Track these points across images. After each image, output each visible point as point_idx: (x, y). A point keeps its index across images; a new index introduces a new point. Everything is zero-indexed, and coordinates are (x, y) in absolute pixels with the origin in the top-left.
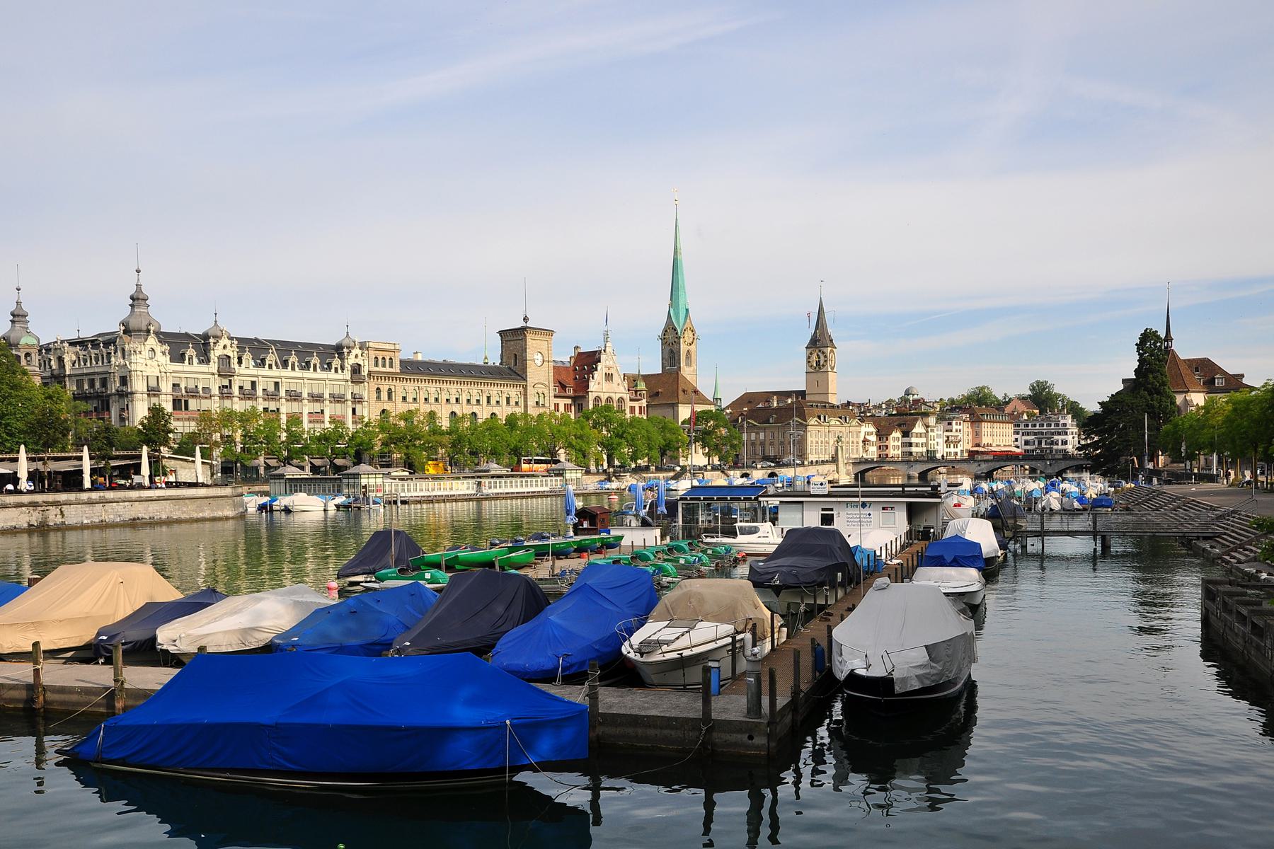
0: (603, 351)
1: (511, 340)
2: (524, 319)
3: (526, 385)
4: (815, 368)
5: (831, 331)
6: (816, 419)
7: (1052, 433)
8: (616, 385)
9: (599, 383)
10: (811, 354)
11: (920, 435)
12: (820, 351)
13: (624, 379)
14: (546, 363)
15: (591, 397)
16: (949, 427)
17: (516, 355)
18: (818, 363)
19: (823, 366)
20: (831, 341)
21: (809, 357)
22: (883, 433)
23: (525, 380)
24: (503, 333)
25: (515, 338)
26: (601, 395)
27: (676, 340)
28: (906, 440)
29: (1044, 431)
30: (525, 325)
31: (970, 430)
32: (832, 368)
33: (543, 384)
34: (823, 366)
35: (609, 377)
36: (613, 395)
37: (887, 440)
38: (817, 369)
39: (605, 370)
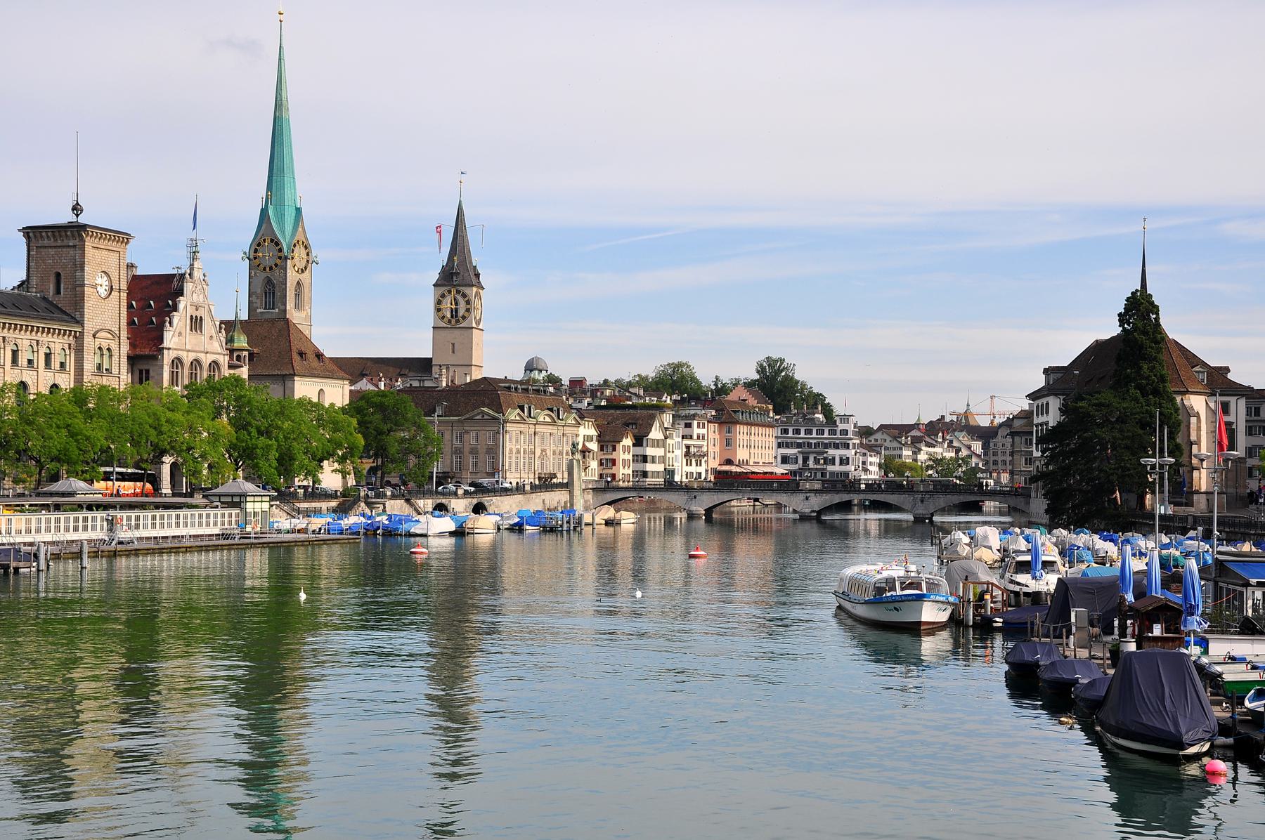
0: (187, 276)
1: (51, 247)
2: (74, 208)
3: (82, 333)
4: (450, 321)
5: (477, 258)
6: (518, 410)
7: (826, 446)
8: (207, 339)
9: (180, 334)
10: (443, 296)
11: (657, 444)
12: (458, 292)
13: (220, 328)
14: (115, 294)
15: (168, 357)
16: (687, 431)
17: (58, 275)
18: (455, 313)
19: (464, 317)
20: (477, 275)
21: (439, 302)
22: (607, 438)
23: (80, 323)
24: (32, 233)
25: (59, 243)
26: (183, 355)
27: (278, 262)
28: (639, 450)
29: (813, 441)
31: (717, 436)
32: (478, 322)
33: (110, 332)
34: (464, 317)
35: (196, 323)
36: (202, 357)
37: (614, 449)
38: (453, 321)
39: (191, 311)
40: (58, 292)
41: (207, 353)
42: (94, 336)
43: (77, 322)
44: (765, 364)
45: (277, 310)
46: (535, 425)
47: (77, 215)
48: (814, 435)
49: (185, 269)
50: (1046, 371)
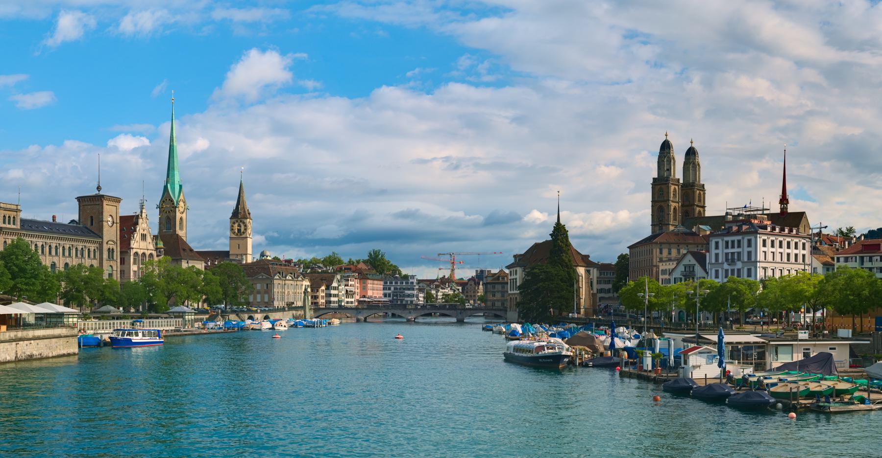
0: (140, 216)
1: (89, 205)
2: (98, 188)
3: (102, 242)
4: (237, 234)
5: (249, 205)
6: (278, 274)
7: (404, 289)
9: (137, 241)
10: (234, 223)
11: (335, 288)
13: (153, 238)
14: (115, 225)
15: (132, 252)
16: (346, 283)
17: (92, 217)
18: (239, 230)
19: (244, 233)
20: (249, 214)
22: (314, 286)
23: (102, 238)
24: (80, 199)
25: (92, 203)
26: (139, 251)
27: (172, 209)
28: (328, 292)
29: (398, 287)
30: (98, 192)
31: (359, 285)
32: (250, 235)
33: (113, 241)
35: (144, 237)
36: (146, 251)
37: (318, 291)
39: (141, 232)
40: (92, 224)
41: (148, 250)
42: (107, 243)
43: (100, 237)
44: (372, 253)
45: (172, 231)
46: (285, 280)
47: (99, 191)
48: (399, 284)
49: (138, 213)
50: (515, 256)
